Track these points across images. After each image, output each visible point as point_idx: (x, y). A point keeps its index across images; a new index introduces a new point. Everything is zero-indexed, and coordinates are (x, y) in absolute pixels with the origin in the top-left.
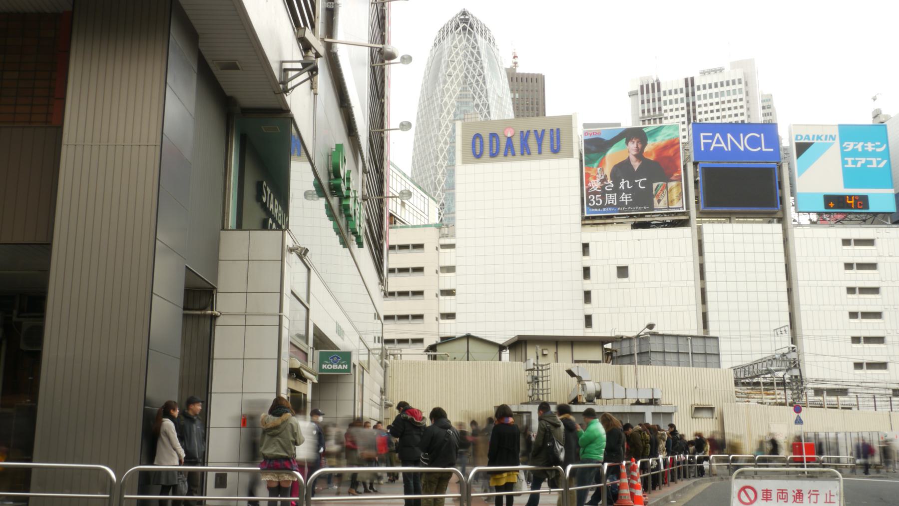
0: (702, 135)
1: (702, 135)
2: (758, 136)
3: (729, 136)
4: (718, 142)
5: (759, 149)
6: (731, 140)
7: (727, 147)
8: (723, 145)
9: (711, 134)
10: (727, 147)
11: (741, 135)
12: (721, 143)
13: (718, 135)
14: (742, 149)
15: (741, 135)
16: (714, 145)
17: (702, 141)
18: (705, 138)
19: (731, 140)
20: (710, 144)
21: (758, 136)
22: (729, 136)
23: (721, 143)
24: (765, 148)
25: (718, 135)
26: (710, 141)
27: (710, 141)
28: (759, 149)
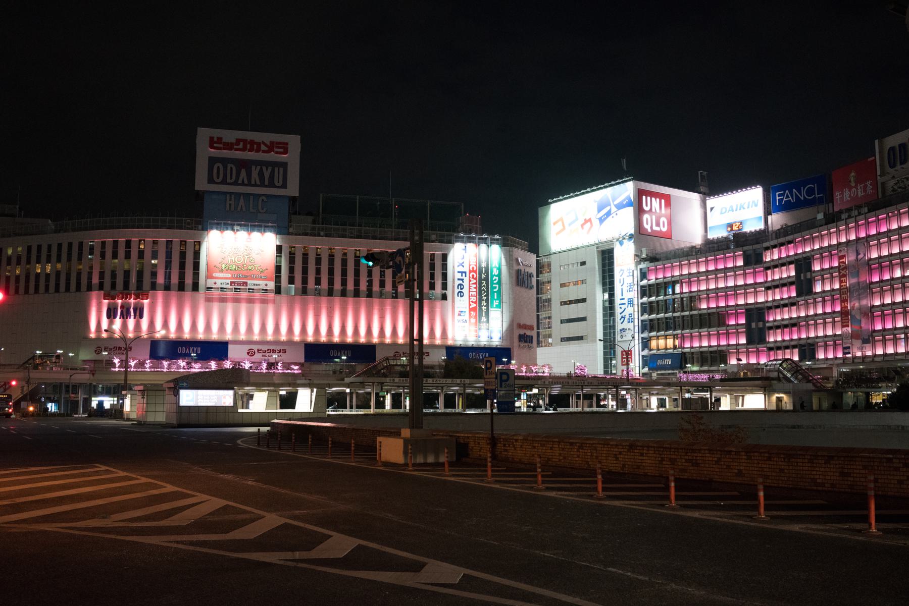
0: (777, 193)
1: (777, 193)
2: (813, 186)
3: (794, 190)
4: (787, 197)
5: (814, 196)
6: (795, 193)
7: (793, 200)
8: (790, 198)
9: (783, 192)
10: (793, 200)
11: (802, 188)
12: (789, 197)
13: (787, 191)
14: (802, 198)
15: (802, 188)
16: (785, 200)
17: (777, 198)
18: (779, 195)
19: (795, 193)
20: (783, 199)
21: (813, 186)
22: (794, 190)
23: (789, 197)
24: (818, 195)
25: (787, 191)
26: (782, 197)
27: (782, 197)
28: (814, 196)
